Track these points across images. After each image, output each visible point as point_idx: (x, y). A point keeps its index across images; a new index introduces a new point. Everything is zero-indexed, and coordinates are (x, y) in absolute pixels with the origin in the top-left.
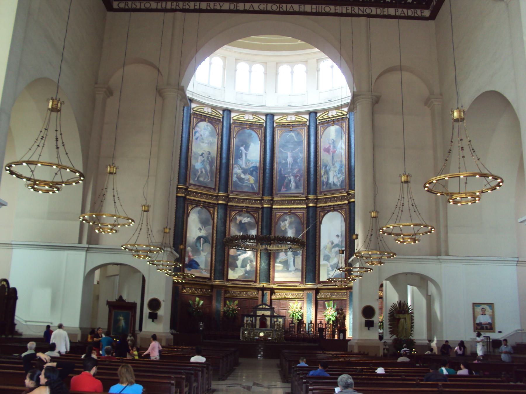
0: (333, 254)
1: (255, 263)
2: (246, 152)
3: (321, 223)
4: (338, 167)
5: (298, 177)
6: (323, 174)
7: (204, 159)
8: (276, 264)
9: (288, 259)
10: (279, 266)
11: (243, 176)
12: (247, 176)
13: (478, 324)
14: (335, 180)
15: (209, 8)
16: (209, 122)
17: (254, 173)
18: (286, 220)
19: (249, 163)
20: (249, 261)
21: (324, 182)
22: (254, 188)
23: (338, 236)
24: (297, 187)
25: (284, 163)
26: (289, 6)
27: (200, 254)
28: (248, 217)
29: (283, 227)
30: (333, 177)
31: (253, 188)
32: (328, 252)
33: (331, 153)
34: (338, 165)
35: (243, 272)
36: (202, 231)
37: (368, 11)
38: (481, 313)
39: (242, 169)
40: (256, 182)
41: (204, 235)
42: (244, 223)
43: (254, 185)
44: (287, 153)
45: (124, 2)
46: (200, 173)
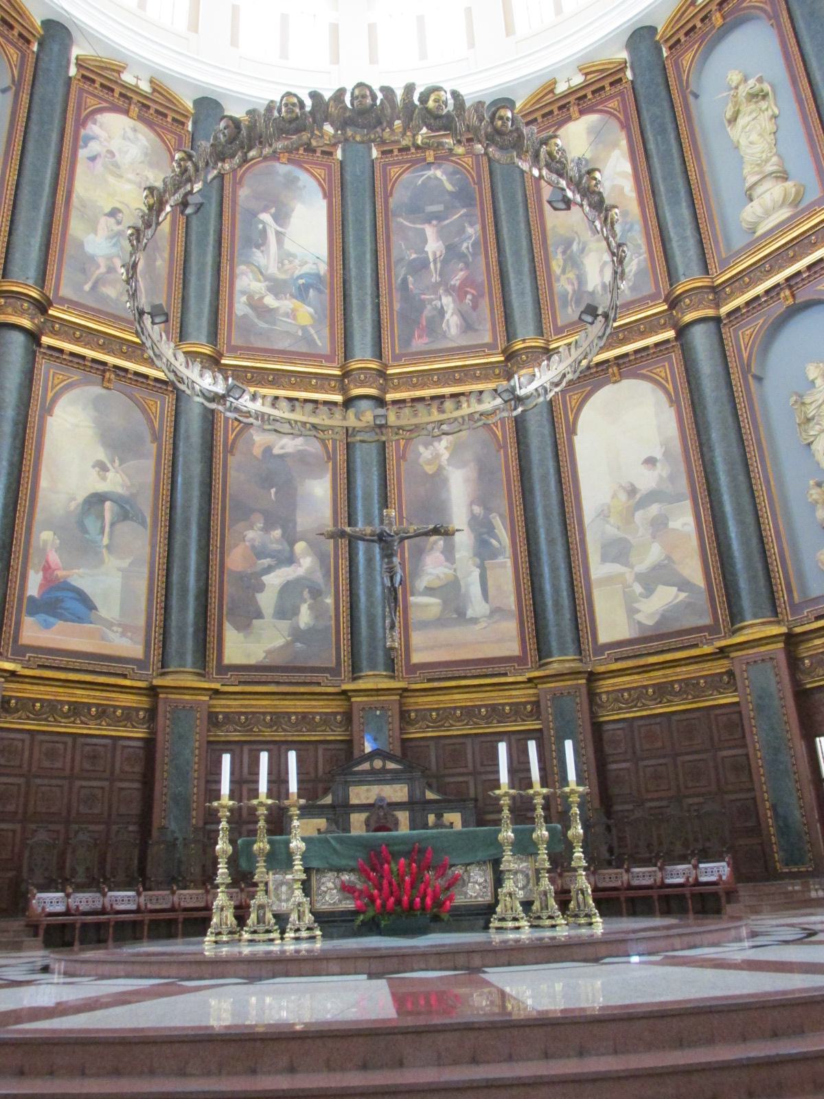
0: (640, 534)
1: (329, 601)
2: (279, 229)
3: (572, 431)
5: (469, 297)
7: (120, 227)
8: (412, 599)
9: (459, 574)
10: (427, 605)
11: (270, 301)
16: (140, 118)
17: (311, 291)
19: (290, 262)
20: (306, 594)
21: (566, 290)
22: (314, 340)
23: (650, 462)
24: (468, 326)
25: (414, 260)
27: (102, 562)
29: (429, 463)
30: (598, 270)
31: (311, 342)
32: (618, 528)
35: (286, 634)
39: (265, 281)
42: (281, 457)
43: (312, 331)
44: (423, 230)
46: (103, 269)
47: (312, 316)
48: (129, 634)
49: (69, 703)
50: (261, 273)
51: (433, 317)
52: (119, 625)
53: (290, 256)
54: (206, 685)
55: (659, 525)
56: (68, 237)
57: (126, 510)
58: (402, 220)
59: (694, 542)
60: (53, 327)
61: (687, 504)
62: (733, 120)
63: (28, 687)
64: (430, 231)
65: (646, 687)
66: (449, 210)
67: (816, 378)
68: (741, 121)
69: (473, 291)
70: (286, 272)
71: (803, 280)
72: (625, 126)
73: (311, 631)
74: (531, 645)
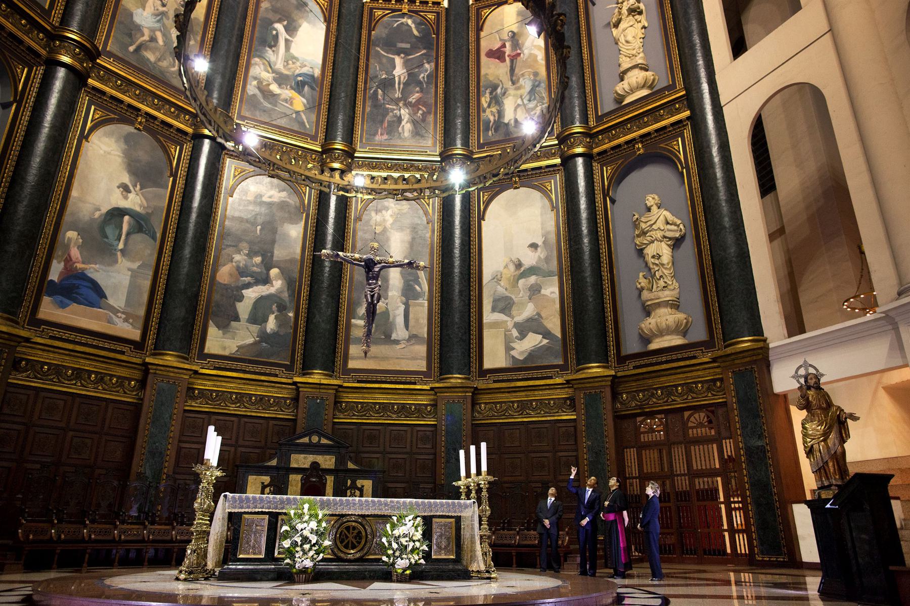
0: (521, 295)
1: (291, 314)
2: (288, 37)
3: (481, 217)
5: (420, 112)
6: (485, 105)
9: (389, 307)
11: (274, 88)
12: (287, 92)
17: (306, 88)
19: (294, 63)
20: (274, 307)
21: (489, 119)
23: (534, 246)
27: (116, 262)
30: (513, 109)
32: (506, 289)
33: (507, 59)
34: (526, 84)
36: (132, 196)
39: (273, 73)
40: (309, 109)
41: (137, 209)
43: (304, 117)
44: (394, 59)
46: (146, 38)
47: (305, 106)
48: (131, 321)
49: (74, 369)
50: (271, 67)
51: (393, 121)
52: (123, 313)
53: (294, 58)
54: (186, 366)
55: (535, 290)
56: (120, 7)
57: (141, 223)
58: (379, 49)
60: (99, 73)
61: (556, 279)
62: (616, 25)
63: (40, 352)
64: (398, 61)
65: (513, 402)
66: (414, 49)
67: (652, 206)
68: (622, 26)
69: (424, 109)
70: (289, 69)
71: (651, 139)
73: (275, 334)
74: (436, 365)
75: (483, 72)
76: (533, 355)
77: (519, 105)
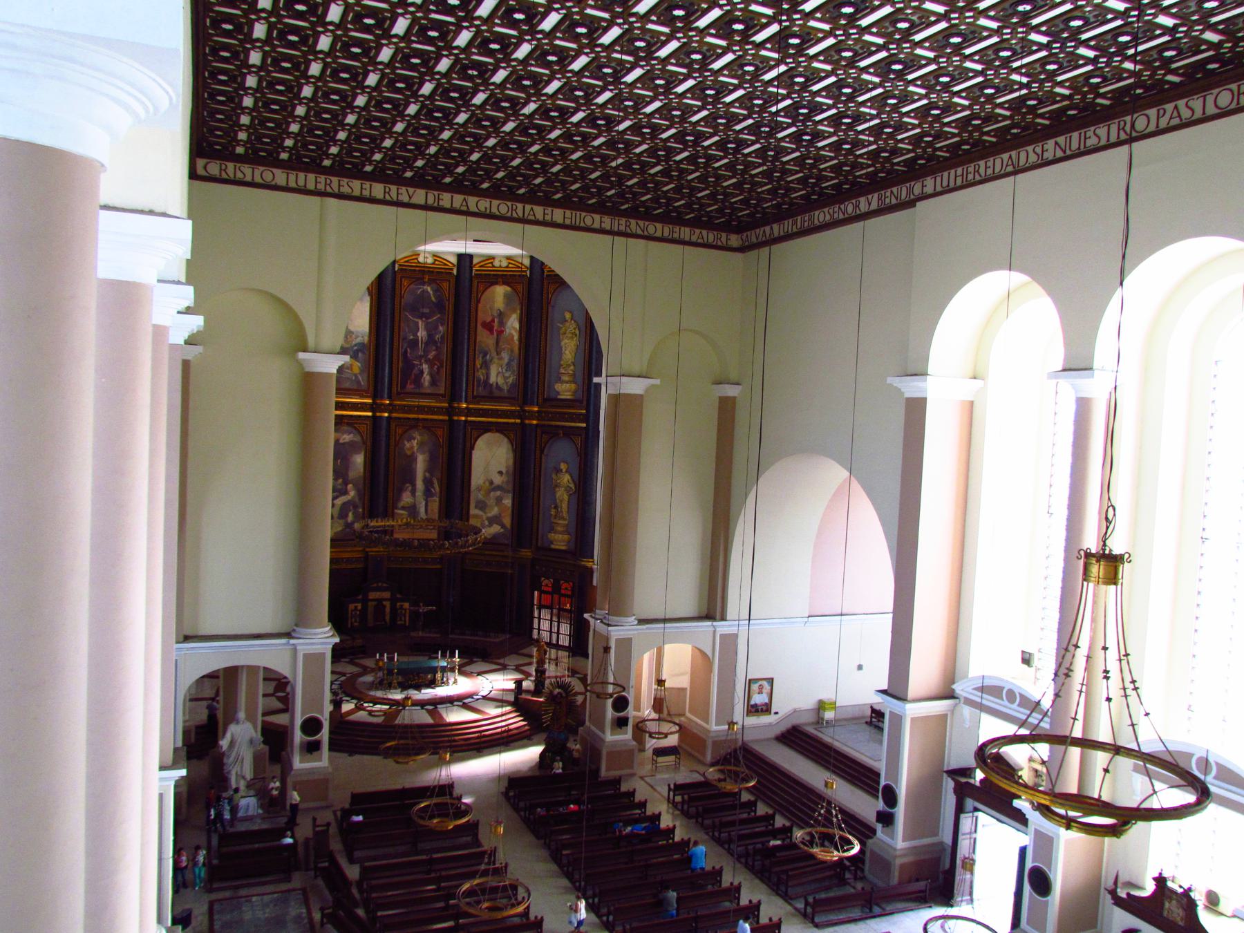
1: (361, 510)
3: (472, 448)
4: (506, 360)
13: (752, 706)
14: (501, 381)
15: (388, 197)
17: (360, 354)
18: (414, 439)
20: (351, 508)
23: (500, 473)
24: (434, 383)
26: (528, 207)
28: (350, 433)
29: (409, 449)
31: (358, 382)
33: (495, 333)
34: (505, 356)
37: (651, 230)
38: (758, 691)
40: (362, 371)
45: (218, 162)
55: (499, 500)
59: (510, 511)
61: (510, 495)
72: (521, 304)
75: (479, 338)
76: (495, 536)
77: (499, 373)
